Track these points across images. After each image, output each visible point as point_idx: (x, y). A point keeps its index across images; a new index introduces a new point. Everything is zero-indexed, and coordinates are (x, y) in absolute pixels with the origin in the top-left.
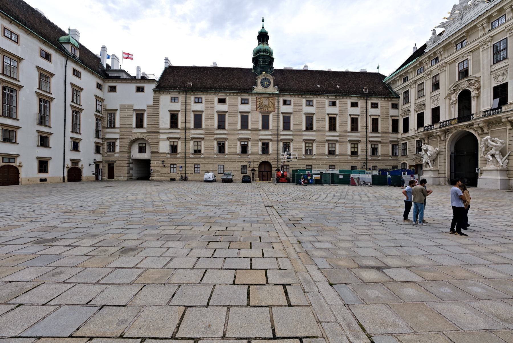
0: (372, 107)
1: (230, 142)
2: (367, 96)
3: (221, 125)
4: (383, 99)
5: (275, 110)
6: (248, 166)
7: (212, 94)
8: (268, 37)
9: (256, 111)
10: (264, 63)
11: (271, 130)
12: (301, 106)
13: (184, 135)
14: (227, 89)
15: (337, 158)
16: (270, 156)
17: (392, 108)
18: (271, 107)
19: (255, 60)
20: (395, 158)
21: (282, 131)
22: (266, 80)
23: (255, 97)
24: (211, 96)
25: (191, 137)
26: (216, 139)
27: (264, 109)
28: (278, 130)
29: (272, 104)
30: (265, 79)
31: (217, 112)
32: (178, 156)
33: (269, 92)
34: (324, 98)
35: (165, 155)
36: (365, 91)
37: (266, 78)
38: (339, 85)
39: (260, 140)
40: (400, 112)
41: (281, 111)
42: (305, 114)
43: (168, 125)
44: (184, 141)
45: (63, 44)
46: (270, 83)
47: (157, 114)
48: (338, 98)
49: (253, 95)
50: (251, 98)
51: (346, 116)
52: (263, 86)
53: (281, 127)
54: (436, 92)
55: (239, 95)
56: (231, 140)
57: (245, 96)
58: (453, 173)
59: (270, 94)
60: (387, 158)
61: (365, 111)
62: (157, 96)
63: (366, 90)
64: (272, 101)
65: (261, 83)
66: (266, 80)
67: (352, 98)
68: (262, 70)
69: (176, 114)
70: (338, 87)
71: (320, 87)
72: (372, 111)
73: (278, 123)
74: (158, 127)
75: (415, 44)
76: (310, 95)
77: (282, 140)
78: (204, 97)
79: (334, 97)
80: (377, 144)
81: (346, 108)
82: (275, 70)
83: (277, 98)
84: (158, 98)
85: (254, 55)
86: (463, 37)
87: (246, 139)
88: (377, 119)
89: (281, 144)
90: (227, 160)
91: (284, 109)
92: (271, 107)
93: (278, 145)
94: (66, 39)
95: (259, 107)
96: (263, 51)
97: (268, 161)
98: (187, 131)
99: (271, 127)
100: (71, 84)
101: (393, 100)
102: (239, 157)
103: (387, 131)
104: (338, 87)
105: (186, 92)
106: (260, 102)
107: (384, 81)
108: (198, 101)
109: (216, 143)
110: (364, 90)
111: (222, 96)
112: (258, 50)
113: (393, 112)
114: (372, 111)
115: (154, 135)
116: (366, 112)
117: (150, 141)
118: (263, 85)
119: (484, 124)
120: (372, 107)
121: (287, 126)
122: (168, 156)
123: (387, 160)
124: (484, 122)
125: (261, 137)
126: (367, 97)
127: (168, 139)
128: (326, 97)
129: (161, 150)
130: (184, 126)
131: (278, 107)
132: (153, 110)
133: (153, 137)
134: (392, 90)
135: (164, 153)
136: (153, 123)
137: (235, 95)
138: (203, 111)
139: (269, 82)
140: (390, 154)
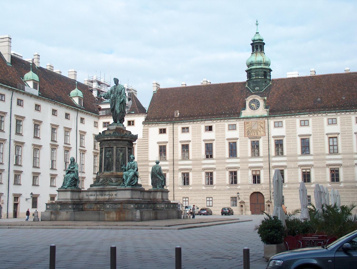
3: (209, 155)
5: (265, 134)
6: (238, 198)
7: (198, 122)
8: (264, 44)
9: (245, 137)
10: (257, 77)
11: (262, 157)
12: (295, 127)
13: (172, 167)
14: (214, 115)
15: (342, 185)
18: (260, 131)
19: (249, 72)
21: (274, 157)
22: (254, 101)
23: (243, 122)
24: (197, 125)
25: (178, 169)
26: (204, 169)
27: (253, 134)
29: (262, 127)
30: (253, 101)
33: (258, 115)
34: (322, 115)
37: (254, 101)
39: (250, 168)
41: (272, 136)
42: (299, 136)
45: (73, 98)
46: (259, 104)
48: (339, 114)
49: (241, 120)
50: (239, 123)
52: (252, 109)
55: (226, 121)
57: (232, 122)
62: (146, 128)
64: (262, 125)
65: (249, 105)
66: (254, 101)
68: (255, 85)
69: (163, 146)
71: (319, 102)
73: (269, 149)
74: (147, 160)
76: (304, 114)
79: (335, 114)
81: (350, 125)
82: (273, 80)
83: (266, 121)
84: (147, 130)
85: (248, 66)
87: (235, 168)
90: (216, 192)
92: (260, 131)
93: (270, 173)
94: (75, 93)
95: (248, 133)
96: (256, 64)
97: (260, 191)
98: (175, 162)
99: (261, 154)
100: (80, 131)
102: (228, 188)
104: (344, 98)
105: (173, 123)
106: (248, 127)
108: (185, 130)
109: (203, 174)
111: (209, 123)
112: (250, 63)
115: (144, 168)
118: (252, 108)
125: (250, 165)
128: (324, 115)
131: (268, 130)
133: (144, 170)
136: (143, 156)
137: (222, 121)
138: (190, 141)
139: (258, 103)
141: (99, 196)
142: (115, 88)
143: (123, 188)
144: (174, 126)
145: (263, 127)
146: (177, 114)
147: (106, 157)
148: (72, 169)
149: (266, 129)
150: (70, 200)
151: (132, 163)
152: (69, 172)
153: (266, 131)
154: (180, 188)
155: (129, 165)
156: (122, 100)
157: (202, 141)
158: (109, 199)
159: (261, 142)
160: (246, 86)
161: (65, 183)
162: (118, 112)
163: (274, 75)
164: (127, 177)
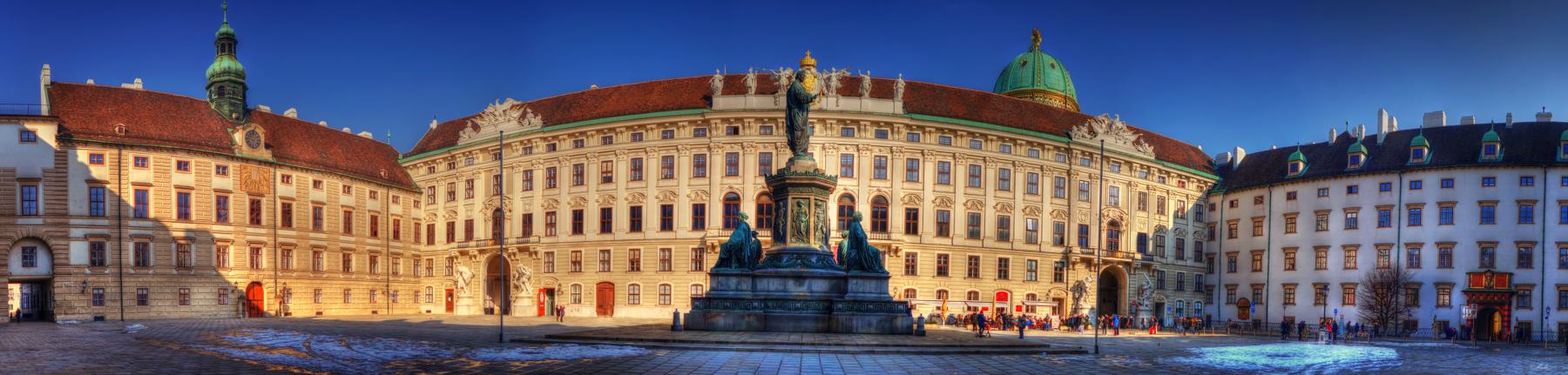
1: (200, 246)
8: (236, 42)
16: (264, 273)
23: (238, 164)
28: (275, 227)
31: (177, 187)
32: (107, 272)
35: (82, 271)
43: (85, 211)
44: (117, 243)
47: (64, 188)
52: (250, 146)
56: (201, 242)
59: (260, 162)
64: (265, 175)
65: (246, 139)
68: (232, 108)
74: (66, 215)
77: (283, 244)
78: (152, 157)
83: (272, 170)
89: (279, 252)
95: (245, 183)
108: (141, 163)
111: (183, 157)
112: (225, 69)
117: (52, 242)
121: (287, 221)
122: (88, 271)
127: (86, 237)
129: (74, 260)
130: (116, 213)
132: (57, 179)
133: (59, 234)
135: (78, 267)
144: (124, 152)
146: (120, 130)
154: (132, 271)
157: (173, 187)
159: (264, 201)
160: (213, 107)
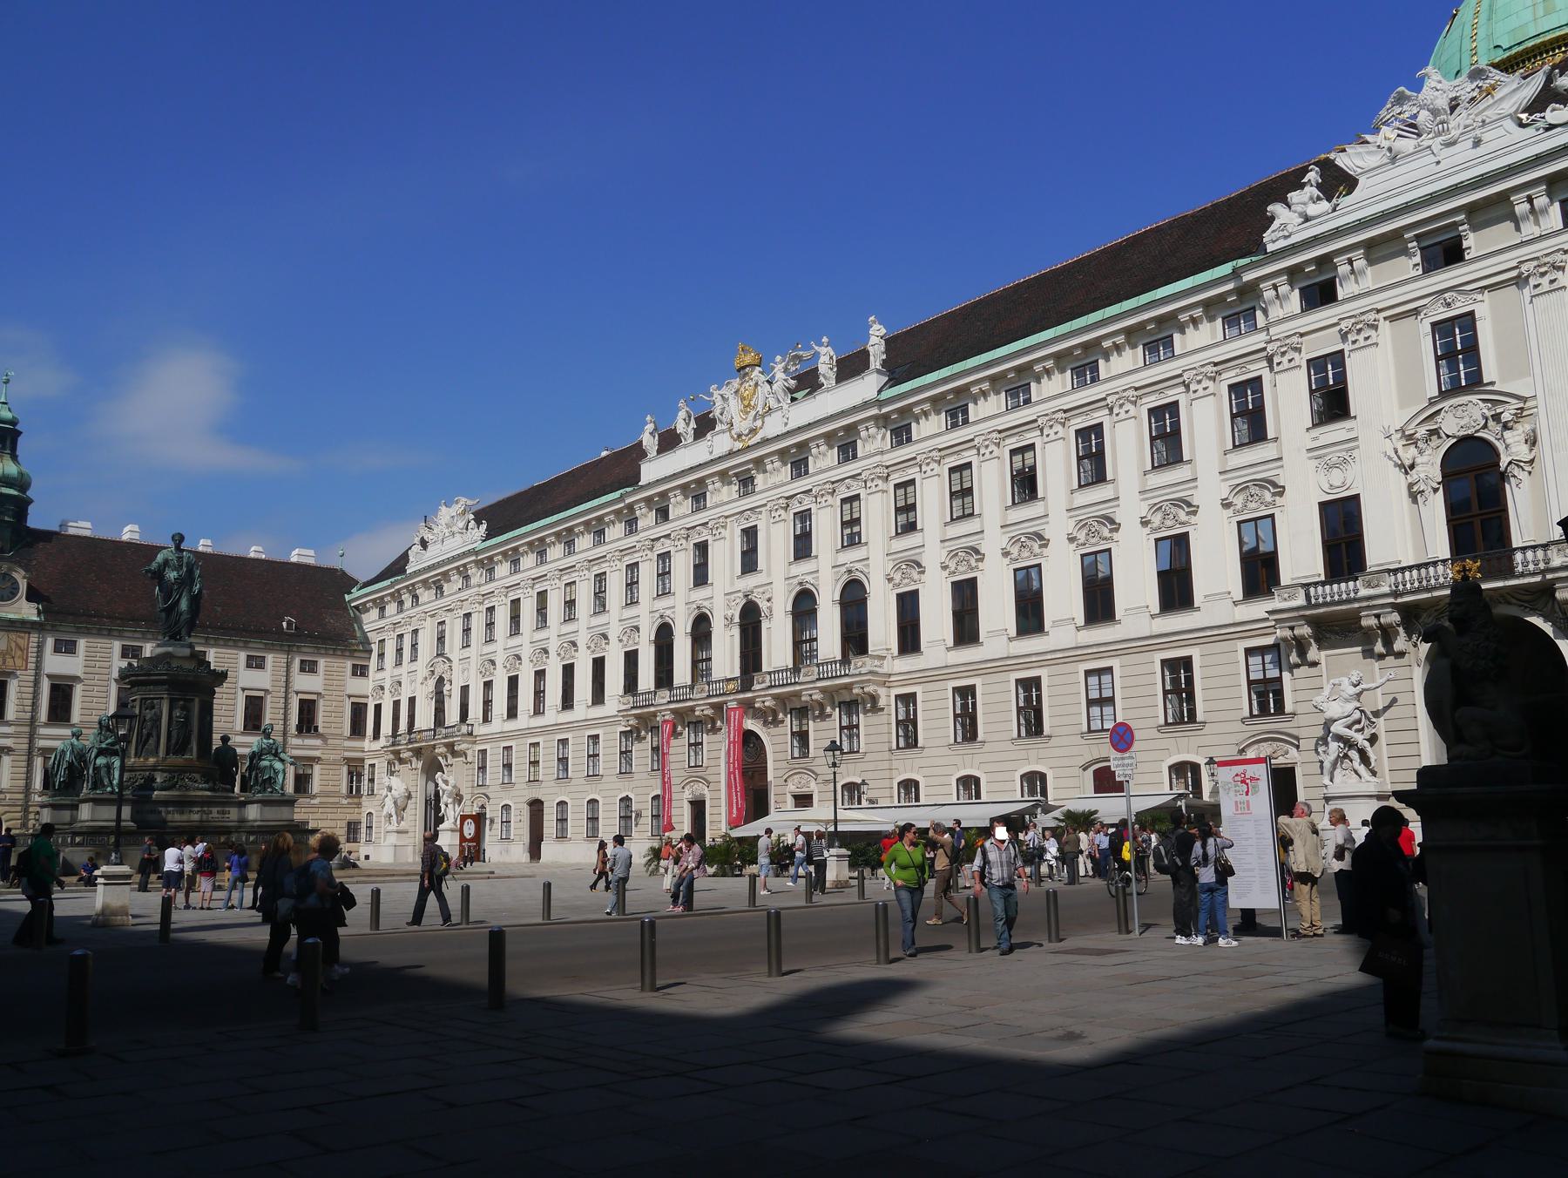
0: (302, 670)
2: (286, 642)
4: (331, 652)
5: (27, 665)
17: (354, 674)
18: (13, 658)
20: (356, 800)
21: (46, 725)
28: (33, 720)
29: (21, 649)
36: (287, 629)
38: (218, 606)
40: (371, 687)
48: (212, 642)
51: (233, 691)
53: (43, 714)
54: (414, 666)
58: (836, 828)
60: (336, 800)
61: (284, 679)
63: (289, 623)
64: (20, 641)
67: (251, 645)
70: (219, 609)
72: (305, 683)
75: (426, 517)
77: (45, 752)
80: (312, 765)
86: (439, 580)
88: (313, 702)
89: (38, 762)
91: (56, 664)
92: (13, 658)
101: (356, 654)
103: (338, 731)
104: (219, 609)
107: (347, 597)
110: (284, 624)
113: (356, 686)
114: (305, 683)
116: (287, 682)
119: (445, 750)
120: (302, 670)
123: (337, 806)
124: (446, 745)
126: (289, 646)
134: (361, 628)
140: (344, 790)
141: (173, 814)
142: (180, 559)
143: (275, 796)
145: (22, 647)
147: (177, 722)
148: (107, 744)
149: (30, 654)
150: (132, 824)
151: (271, 741)
152: (101, 752)
153: (30, 659)
155: (264, 746)
156: (196, 589)
158: (201, 821)
161: (106, 782)
162: (184, 617)
163: (37, 519)
164: (276, 773)
